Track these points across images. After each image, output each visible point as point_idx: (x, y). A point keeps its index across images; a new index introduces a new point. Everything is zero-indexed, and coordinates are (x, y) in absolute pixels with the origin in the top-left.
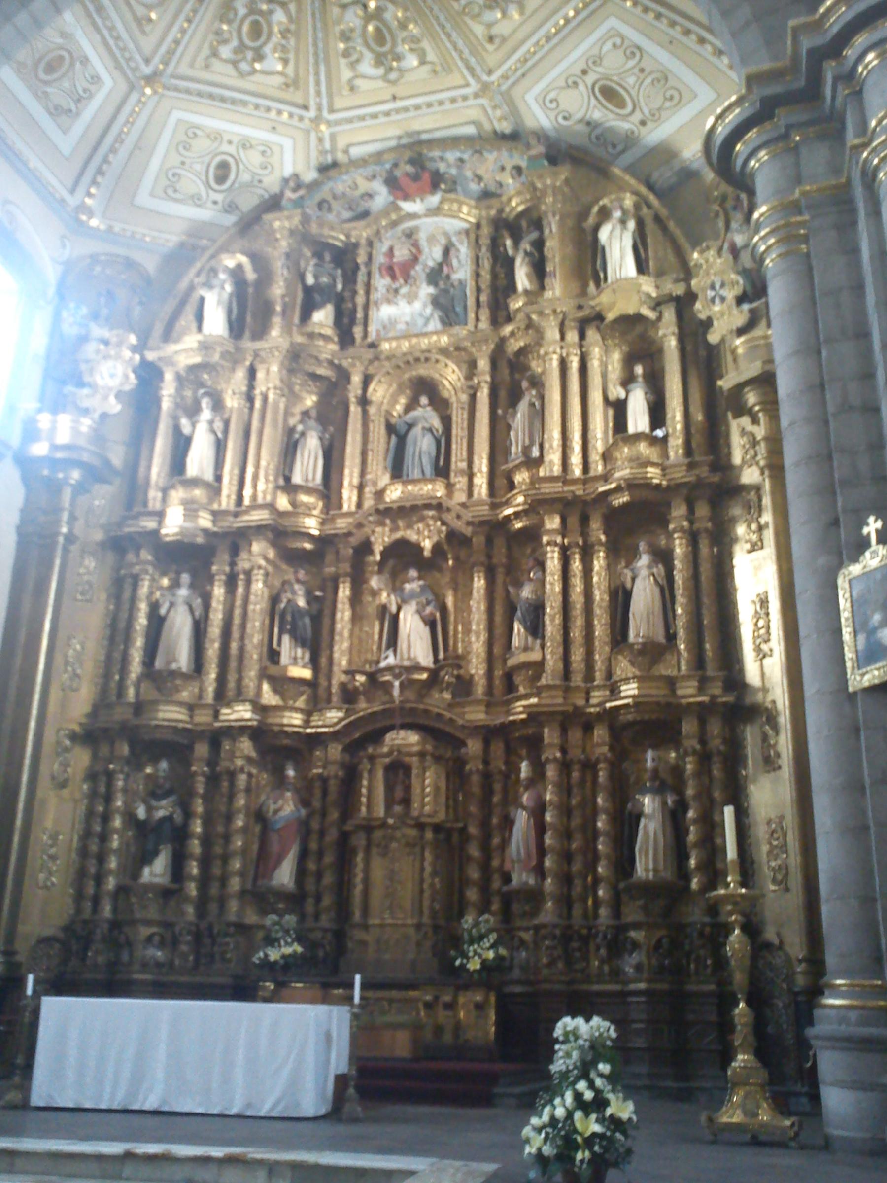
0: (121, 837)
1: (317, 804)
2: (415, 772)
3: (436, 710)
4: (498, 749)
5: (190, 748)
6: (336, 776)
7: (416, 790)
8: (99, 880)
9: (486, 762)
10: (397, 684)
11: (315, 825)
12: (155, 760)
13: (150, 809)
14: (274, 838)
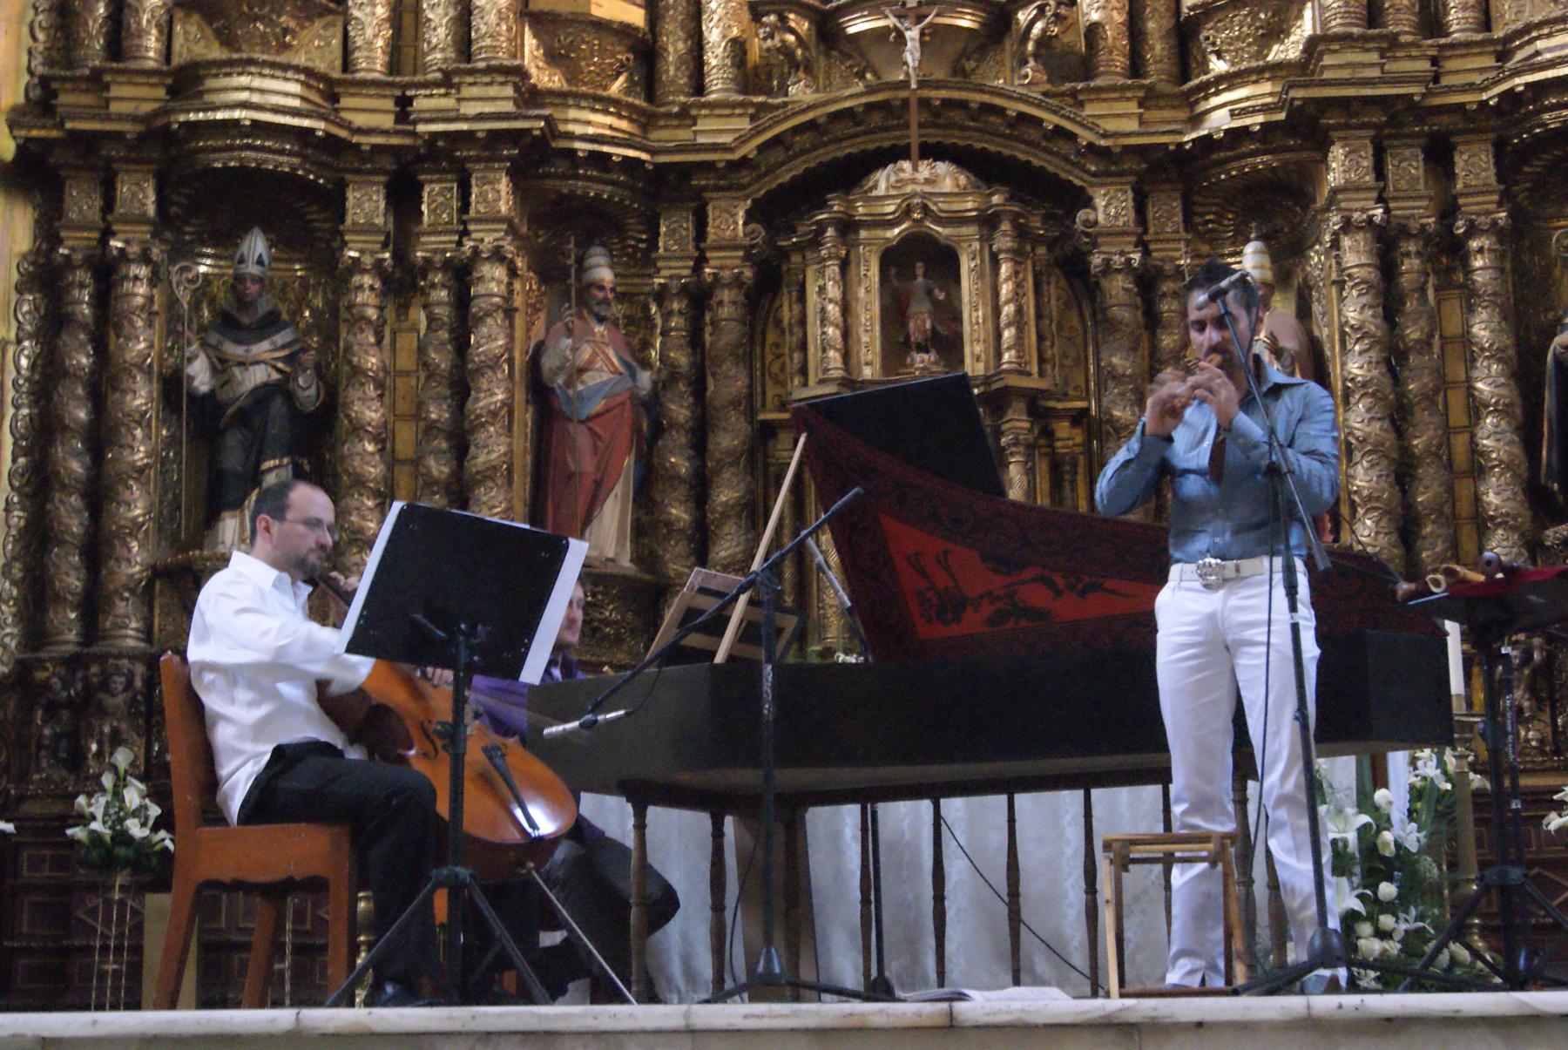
0: (148, 436)
1: (682, 359)
2: (966, 264)
3: (1014, 108)
4: (1167, 212)
5: (334, 202)
6: (737, 281)
7: (973, 316)
8: (97, 551)
9: (1143, 245)
10: (913, 34)
11: (679, 410)
12: (226, 239)
13: (221, 366)
14: (582, 439)
